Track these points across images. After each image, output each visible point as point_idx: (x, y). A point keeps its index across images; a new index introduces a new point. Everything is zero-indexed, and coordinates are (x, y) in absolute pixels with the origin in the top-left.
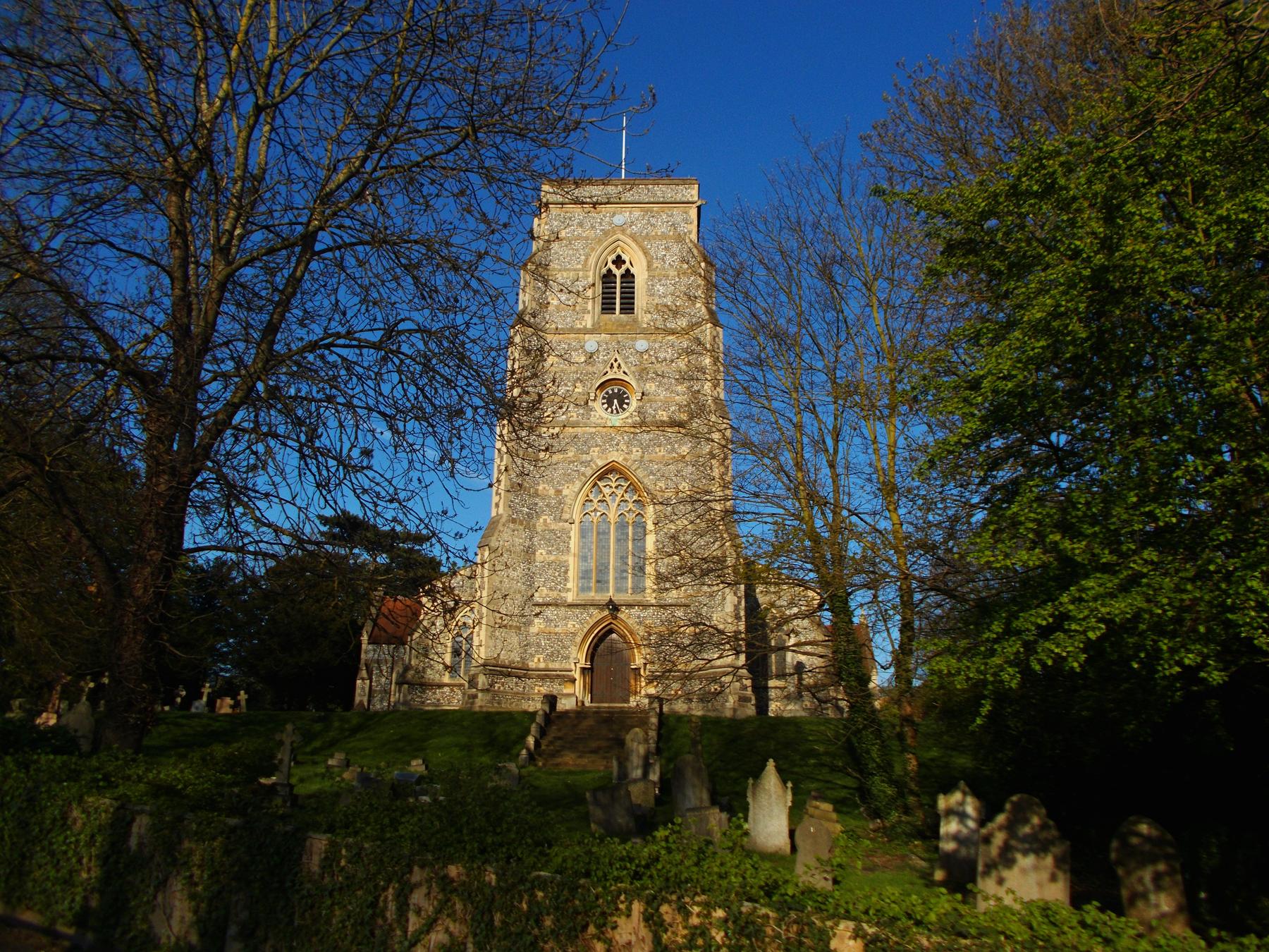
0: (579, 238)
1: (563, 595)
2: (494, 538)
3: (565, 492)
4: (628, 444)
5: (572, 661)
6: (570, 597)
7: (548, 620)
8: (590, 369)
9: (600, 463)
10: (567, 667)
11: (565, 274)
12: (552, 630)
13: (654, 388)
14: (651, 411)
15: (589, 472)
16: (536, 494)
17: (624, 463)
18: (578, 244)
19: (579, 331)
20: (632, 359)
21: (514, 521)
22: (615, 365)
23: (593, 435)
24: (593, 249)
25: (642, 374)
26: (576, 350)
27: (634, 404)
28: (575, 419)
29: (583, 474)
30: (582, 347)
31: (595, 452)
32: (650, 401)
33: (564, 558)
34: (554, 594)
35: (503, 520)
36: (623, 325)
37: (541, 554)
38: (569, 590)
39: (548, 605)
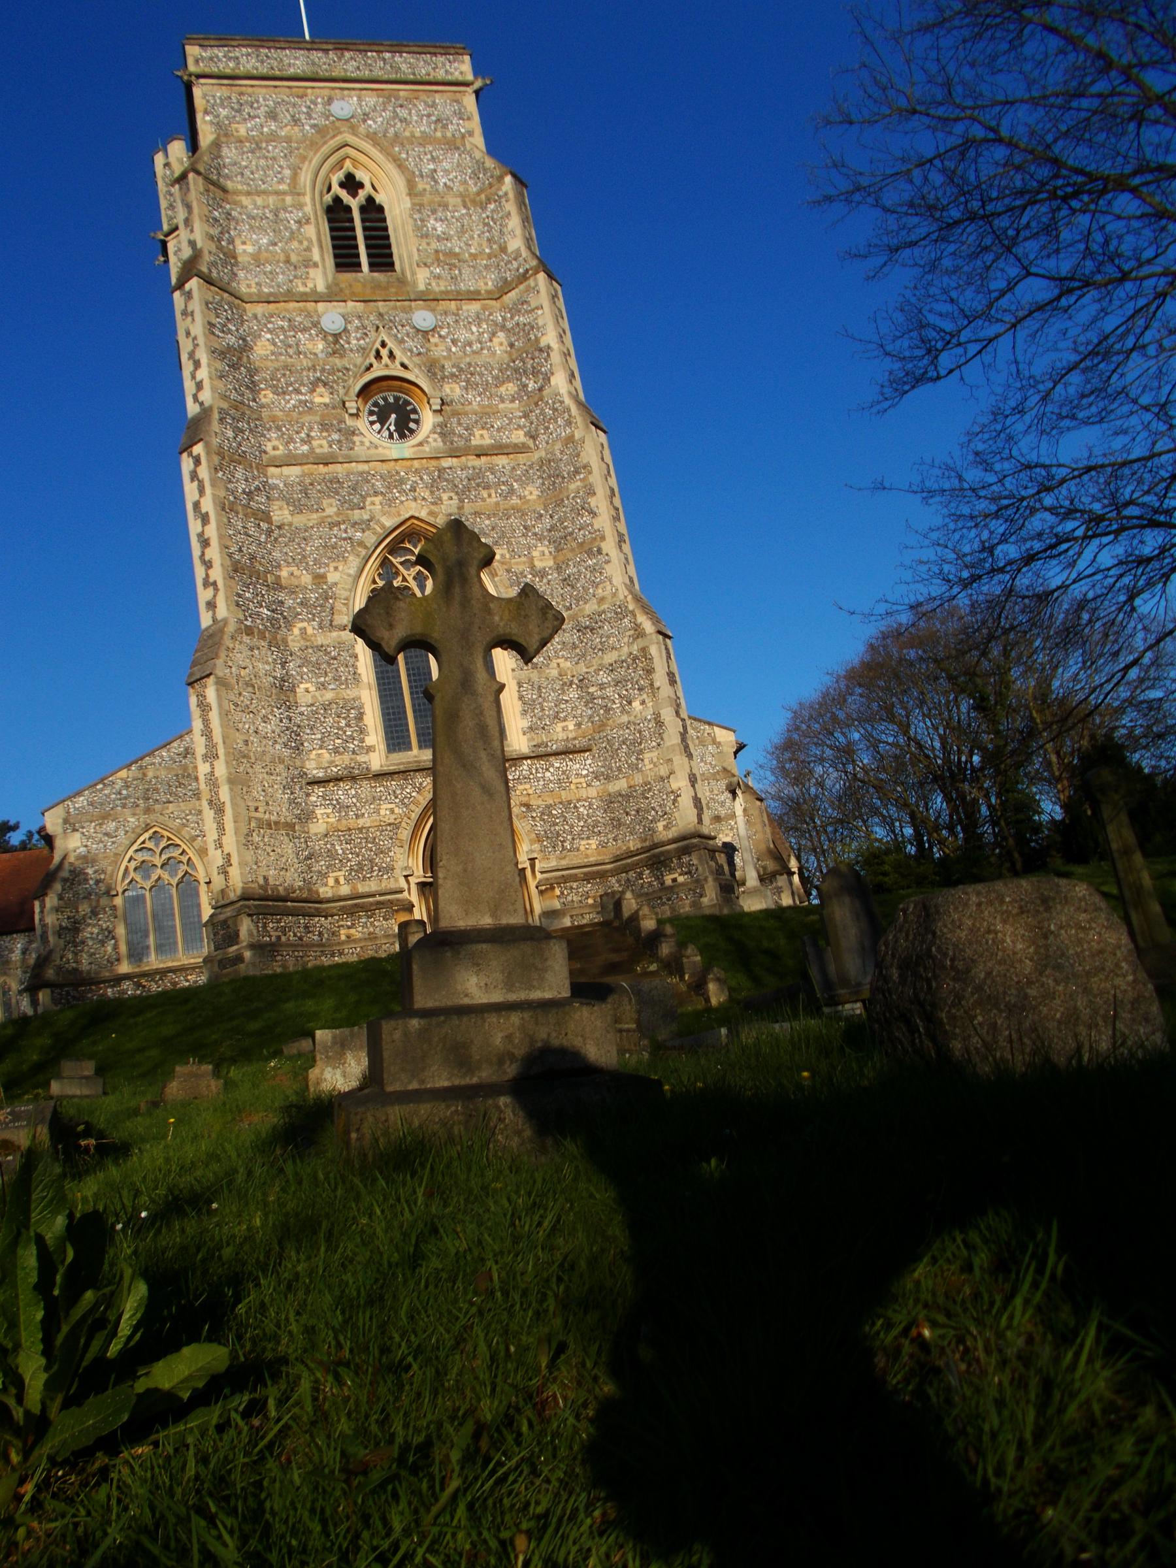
0: (273, 137)
1: (361, 758)
2: (219, 662)
3: (332, 577)
4: (433, 487)
5: (399, 874)
6: (377, 760)
7: (341, 807)
8: (338, 362)
9: (389, 523)
10: (392, 885)
11: (259, 201)
12: (352, 823)
13: (458, 390)
14: (459, 430)
15: (371, 539)
16: (278, 585)
17: (431, 520)
18: (274, 149)
19: (304, 298)
20: (410, 343)
21: (249, 631)
22: (384, 353)
23: (365, 477)
24: (303, 158)
25: (433, 368)
26: (305, 330)
27: (428, 419)
28: (326, 450)
29: (361, 544)
30: (316, 324)
31: (375, 504)
32: (455, 413)
33: (350, 693)
34: (344, 760)
35: (231, 628)
36: (377, 286)
37: (306, 692)
38: (370, 749)
39: (338, 779)
